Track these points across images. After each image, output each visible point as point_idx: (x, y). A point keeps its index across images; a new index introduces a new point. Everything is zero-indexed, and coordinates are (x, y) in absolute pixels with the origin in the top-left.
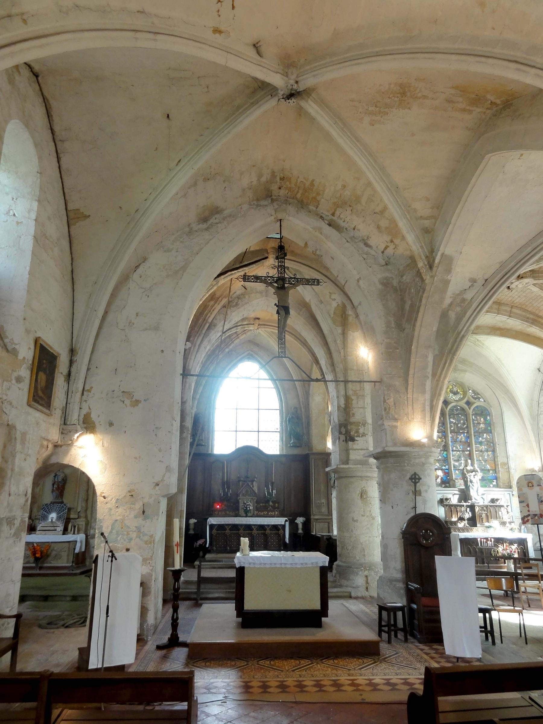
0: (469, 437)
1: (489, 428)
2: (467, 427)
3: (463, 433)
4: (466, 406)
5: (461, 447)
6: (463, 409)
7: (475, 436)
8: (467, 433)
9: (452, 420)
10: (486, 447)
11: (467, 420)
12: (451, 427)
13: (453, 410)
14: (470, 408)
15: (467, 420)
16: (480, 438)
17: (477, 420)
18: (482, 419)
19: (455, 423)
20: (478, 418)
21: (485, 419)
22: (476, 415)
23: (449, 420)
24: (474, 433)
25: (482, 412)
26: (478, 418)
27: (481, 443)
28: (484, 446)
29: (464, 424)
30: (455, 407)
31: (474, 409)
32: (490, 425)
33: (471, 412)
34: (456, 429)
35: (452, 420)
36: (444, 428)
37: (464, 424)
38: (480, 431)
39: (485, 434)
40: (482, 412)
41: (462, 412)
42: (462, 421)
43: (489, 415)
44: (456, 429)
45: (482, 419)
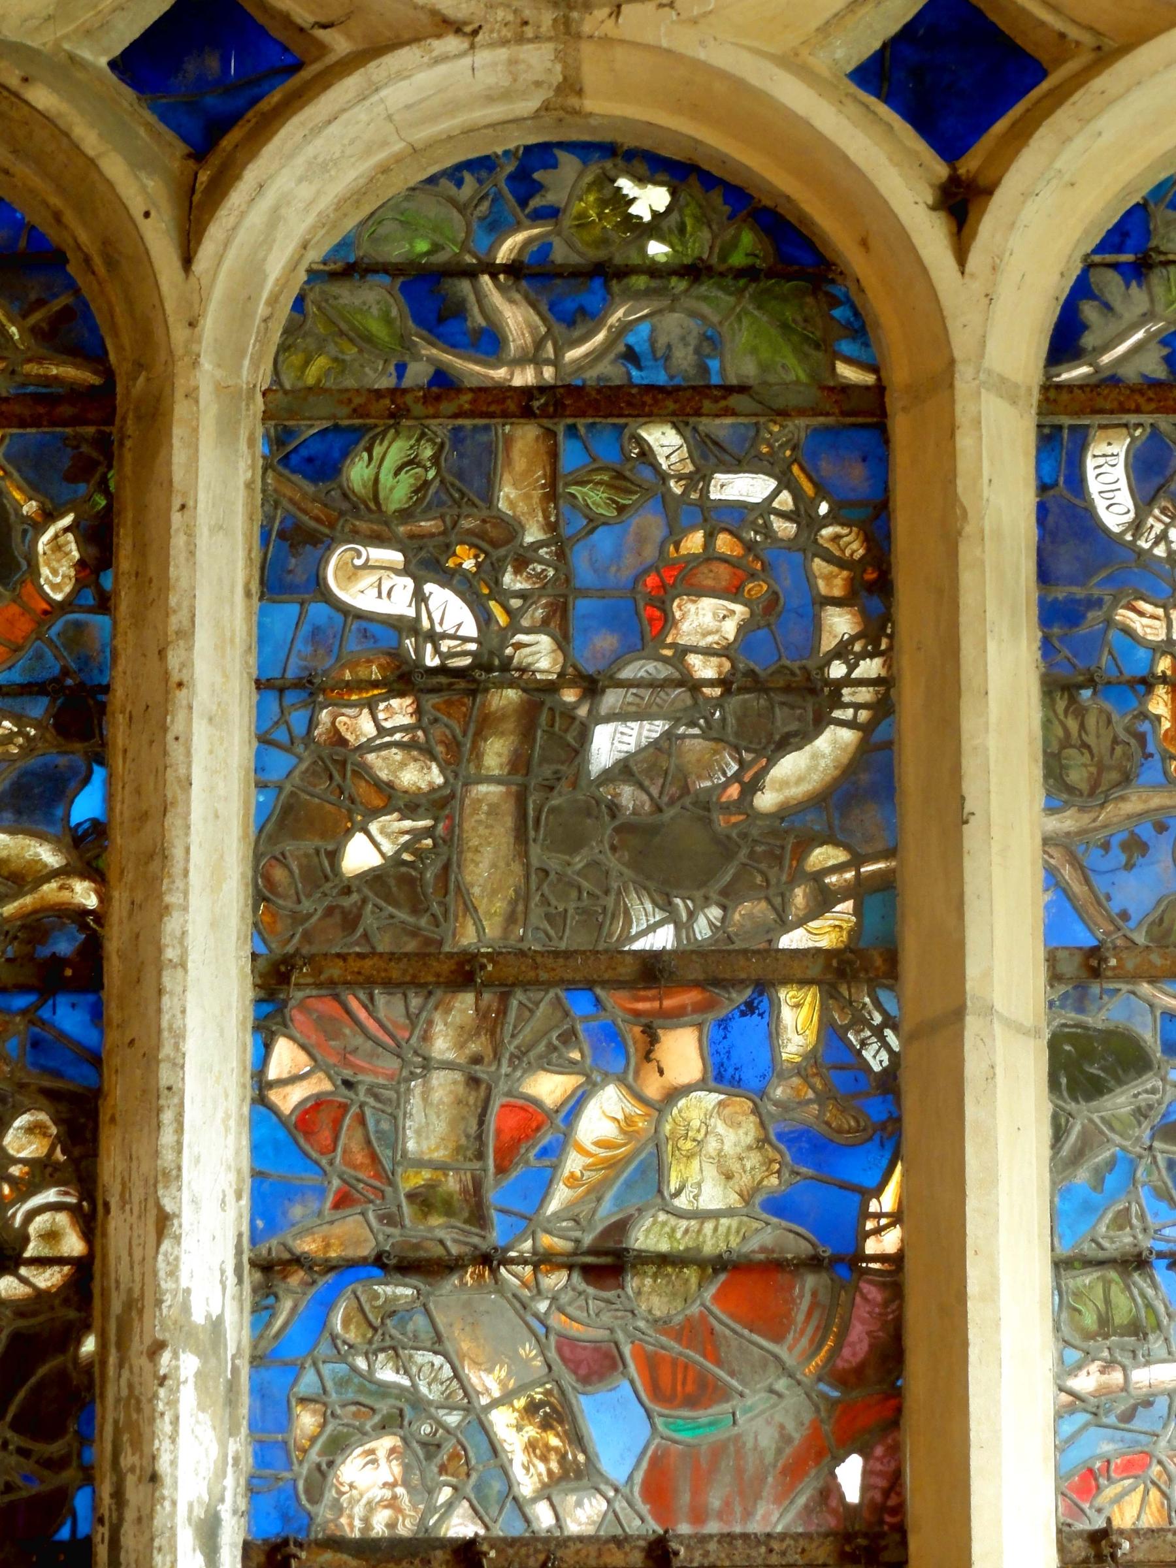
0: (877, 1118)
2: (864, 791)
3: (733, 981)
4: (889, 164)
5: (618, 1428)
6: (779, 251)
8: (836, 973)
9: (371, 583)
12: (307, 799)
13: (433, 294)
14: (961, 203)
19: (452, 693)
23: (288, 560)
24: (1081, 970)
29: (776, 691)
30: (516, 176)
33: (998, 296)
34: (488, 867)
35: (371, 583)
36: (89, 850)
37: (776, 691)
41: (752, 347)
42: (707, 621)
44: (488, 867)
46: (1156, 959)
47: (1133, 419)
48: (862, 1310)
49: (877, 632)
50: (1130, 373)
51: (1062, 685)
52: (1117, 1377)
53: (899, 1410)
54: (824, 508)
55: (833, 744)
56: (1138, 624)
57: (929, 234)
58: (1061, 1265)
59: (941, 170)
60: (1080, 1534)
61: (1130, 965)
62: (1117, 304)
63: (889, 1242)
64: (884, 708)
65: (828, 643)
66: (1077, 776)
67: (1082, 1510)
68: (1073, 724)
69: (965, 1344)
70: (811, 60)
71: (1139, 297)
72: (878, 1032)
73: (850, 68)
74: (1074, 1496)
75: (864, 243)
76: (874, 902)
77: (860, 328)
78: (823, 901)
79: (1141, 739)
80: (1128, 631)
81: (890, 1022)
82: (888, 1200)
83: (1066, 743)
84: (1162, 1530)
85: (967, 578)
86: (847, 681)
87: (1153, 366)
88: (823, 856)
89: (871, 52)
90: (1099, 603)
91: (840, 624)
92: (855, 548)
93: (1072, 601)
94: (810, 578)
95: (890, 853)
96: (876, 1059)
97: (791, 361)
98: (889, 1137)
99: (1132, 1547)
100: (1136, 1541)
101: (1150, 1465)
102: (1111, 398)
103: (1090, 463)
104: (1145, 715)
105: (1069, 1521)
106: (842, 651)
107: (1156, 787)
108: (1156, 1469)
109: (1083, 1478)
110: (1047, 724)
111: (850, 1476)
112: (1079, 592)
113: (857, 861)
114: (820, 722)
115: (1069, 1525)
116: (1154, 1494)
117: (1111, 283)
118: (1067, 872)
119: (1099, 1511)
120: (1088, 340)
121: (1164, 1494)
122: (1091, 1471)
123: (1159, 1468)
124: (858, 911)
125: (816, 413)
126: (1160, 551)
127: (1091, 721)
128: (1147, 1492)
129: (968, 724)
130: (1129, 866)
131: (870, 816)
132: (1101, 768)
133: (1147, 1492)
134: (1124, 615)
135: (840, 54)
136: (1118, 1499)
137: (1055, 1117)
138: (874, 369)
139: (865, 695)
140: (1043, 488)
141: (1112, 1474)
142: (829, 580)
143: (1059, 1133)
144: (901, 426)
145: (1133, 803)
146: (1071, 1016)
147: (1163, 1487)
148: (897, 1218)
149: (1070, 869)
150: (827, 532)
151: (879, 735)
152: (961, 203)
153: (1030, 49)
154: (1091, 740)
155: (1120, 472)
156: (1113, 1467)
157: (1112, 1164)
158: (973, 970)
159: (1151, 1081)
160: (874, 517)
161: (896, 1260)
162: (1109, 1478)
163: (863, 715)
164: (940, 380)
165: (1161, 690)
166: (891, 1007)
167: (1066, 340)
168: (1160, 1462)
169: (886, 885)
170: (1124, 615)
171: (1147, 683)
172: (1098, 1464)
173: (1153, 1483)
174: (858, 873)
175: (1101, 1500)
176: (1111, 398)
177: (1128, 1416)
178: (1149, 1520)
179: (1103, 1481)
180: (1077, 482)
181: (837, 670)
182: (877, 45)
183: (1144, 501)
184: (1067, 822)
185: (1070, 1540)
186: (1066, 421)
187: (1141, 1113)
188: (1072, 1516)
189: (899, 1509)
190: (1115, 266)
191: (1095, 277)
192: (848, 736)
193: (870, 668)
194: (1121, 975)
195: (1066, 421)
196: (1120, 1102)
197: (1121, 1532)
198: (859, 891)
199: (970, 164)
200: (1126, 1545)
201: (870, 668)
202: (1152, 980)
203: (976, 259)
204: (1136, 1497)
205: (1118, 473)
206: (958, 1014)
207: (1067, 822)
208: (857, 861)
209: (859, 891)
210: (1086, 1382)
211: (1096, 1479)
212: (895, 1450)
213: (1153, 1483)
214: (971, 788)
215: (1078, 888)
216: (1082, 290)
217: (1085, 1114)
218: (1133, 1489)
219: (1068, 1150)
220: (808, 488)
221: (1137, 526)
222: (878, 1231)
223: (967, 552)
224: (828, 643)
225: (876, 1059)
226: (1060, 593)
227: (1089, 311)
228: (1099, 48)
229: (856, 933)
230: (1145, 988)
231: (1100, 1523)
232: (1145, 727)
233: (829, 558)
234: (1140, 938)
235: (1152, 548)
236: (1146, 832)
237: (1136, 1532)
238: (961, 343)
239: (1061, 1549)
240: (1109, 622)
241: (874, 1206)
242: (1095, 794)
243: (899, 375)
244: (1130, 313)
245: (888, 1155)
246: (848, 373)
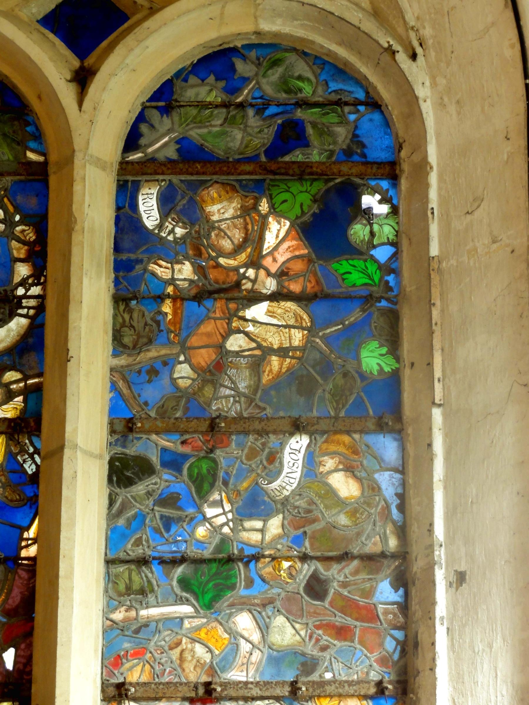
1: (373, 358)
7: (123, 472)
10: (285, 633)
11: (38, 256)
14: (82, 79)
15: (38, 256)
16: (218, 513)
17: (196, 246)
18: (276, 231)
20: (222, 210)
21: (327, 227)
22: (192, 169)
24: (123, 427)
25: (291, 135)
26: (222, 210)
27: (214, 577)
28: (261, 608)
31: (164, 97)
32: (386, 309)
38: (225, 402)
39: (299, 443)
40: (291, 135)
43: (391, 171)
45: (276, 231)
46: (159, 424)
47: (161, 177)
48: (18, 582)
49: (39, 275)
50: (161, 156)
51: (121, 299)
52: (133, 613)
53: (32, 628)
54: (17, 218)
55: (18, 325)
56: (159, 271)
57: (66, 93)
58: (109, 562)
59: (76, 63)
60: (112, 684)
61: (147, 426)
62: (157, 125)
63: (32, 551)
64: (41, 309)
65: (17, 279)
66: (127, 340)
67: (114, 674)
68: (127, 316)
69: (58, 598)
70: (20, 13)
71: (167, 122)
72: (31, 456)
73: (40, 17)
74: (111, 667)
75: (39, 97)
76: (32, 397)
77: (38, 136)
78: (10, 396)
79: (158, 323)
80: (154, 274)
81: (37, 451)
82: (32, 533)
83: (123, 325)
84: (150, 683)
85: (75, 250)
86: (25, 296)
87: (172, 153)
88: (11, 376)
89: (51, 9)
90: (139, 261)
91: (23, 270)
92: (31, 236)
93: (129, 260)
94: (9, 250)
95: (40, 375)
96: (30, 468)
97: (6, 150)
98: (32, 504)
99: (135, 691)
100: (138, 688)
101: (146, 654)
102: (152, 168)
103: (140, 198)
104: (160, 313)
105: (108, 678)
106: (23, 283)
107: (164, 345)
108: (148, 655)
109: (115, 659)
110: (115, 317)
111: (9, 657)
112: (133, 256)
113: (25, 378)
114: (12, 315)
115: (108, 681)
116: (147, 666)
117: (154, 116)
118: (121, 384)
119: (122, 674)
120: (143, 141)
121: (151, 666)
122: (119, 656)
123: (150, 655)
124: (25, 401)
125: (15, 174)
126: (170, 238)
127: (135, 315)
128: (144, 665)
129: (72, 315)
130: (149, 381)
131: (32, 358)
132: (139, 336)
133: (144, 665)
134: (153, 267)
135: (34, 10)
136: (131, 669)
137: (110, 495)
138: (44, 154)
139: (32, 303)
140: (119, 208)
141: (129, 658)
142: (18, 250)
143: (111, 502)
144: (53, 180)
145: (153, 353)
146: (119, 449)
147: (152, 663)
148: (35, 541)
149: (123, 383)
150: (19, 228)
151: (39, 320)
152: (82, 79)
153: (122, 8)
154: (135, 324)
155: (154, 202)
156: (129, 654)
157: (135, 516)
158: (69, 428)
159: (154, 479)
160: (40, 222)
161: (33, 559)
162: (127, 660)
163: (32, 312)
164: (68, 161)
165: (168, 302)
166: (38, 445)
167: (132, 141)
168: (151, 652)
169: (38, 389)
170: (153, 267)
171: (161, 298)
172: (122, 653)
173: (147, 661)
174: (26, 384)
175: (121, 670)
176: (152, 168)
177: (137, 631)
178: (144, 678)
179: (124, 661)
180: (134, 206)
181: (21, 291)
182: (53, 6)
183: (164, 215)
184: (122, 361)
185: (107, 687)
186: (130, 178)
187: (149, 494)
188: (110, 677)
189: (30, 673)
190: (157, 108)
191: (147, 113)
192: (24, 321)
193: (35, 290)
194: (142, 431)
195: (130, 178)
196: (140, 488)
197: (131, 684)
198: (26, 392)
199: (90, 61)
200: (133, 690)
201: (35, 290)
202: (157, 433)
203: (86, 104)
204: (139, 668)
205: (153, 202)
206: (61, 448)
207: (122, 361)
208: (25, 378)
209: (26, 392)
210: (118, 616)
211: (121, 660)
212: (30, 646)
213: (147, 661)
214: (72, 345)
215: (125, 391)
216: (141, 118)
217: (123, 494)
218: (138, 664)
219: (114, 510)
220: (11, 208)
221: (160, 226)
222: (27, 546)
223: (76, 238)
224: (17, 279)
225: (30, 468)
226: (124, 257)
227: (144, 128)
228: (151, 8)
229: (24, 411)
230: (154, 437)
231: (121, 680)
232: (160, 318)
233: (19, 240)
234: (153, 414)
235: (167, 236)
236: (158, 366)
237: (138, 684)
238: (78, 143)
239: (103, 691)
240: (145, 270)
241: (26, 535)
242: (136, 348)
243: (53, 157)
244: (163, 129)
245: (33, 511)
246: (32, 156)
